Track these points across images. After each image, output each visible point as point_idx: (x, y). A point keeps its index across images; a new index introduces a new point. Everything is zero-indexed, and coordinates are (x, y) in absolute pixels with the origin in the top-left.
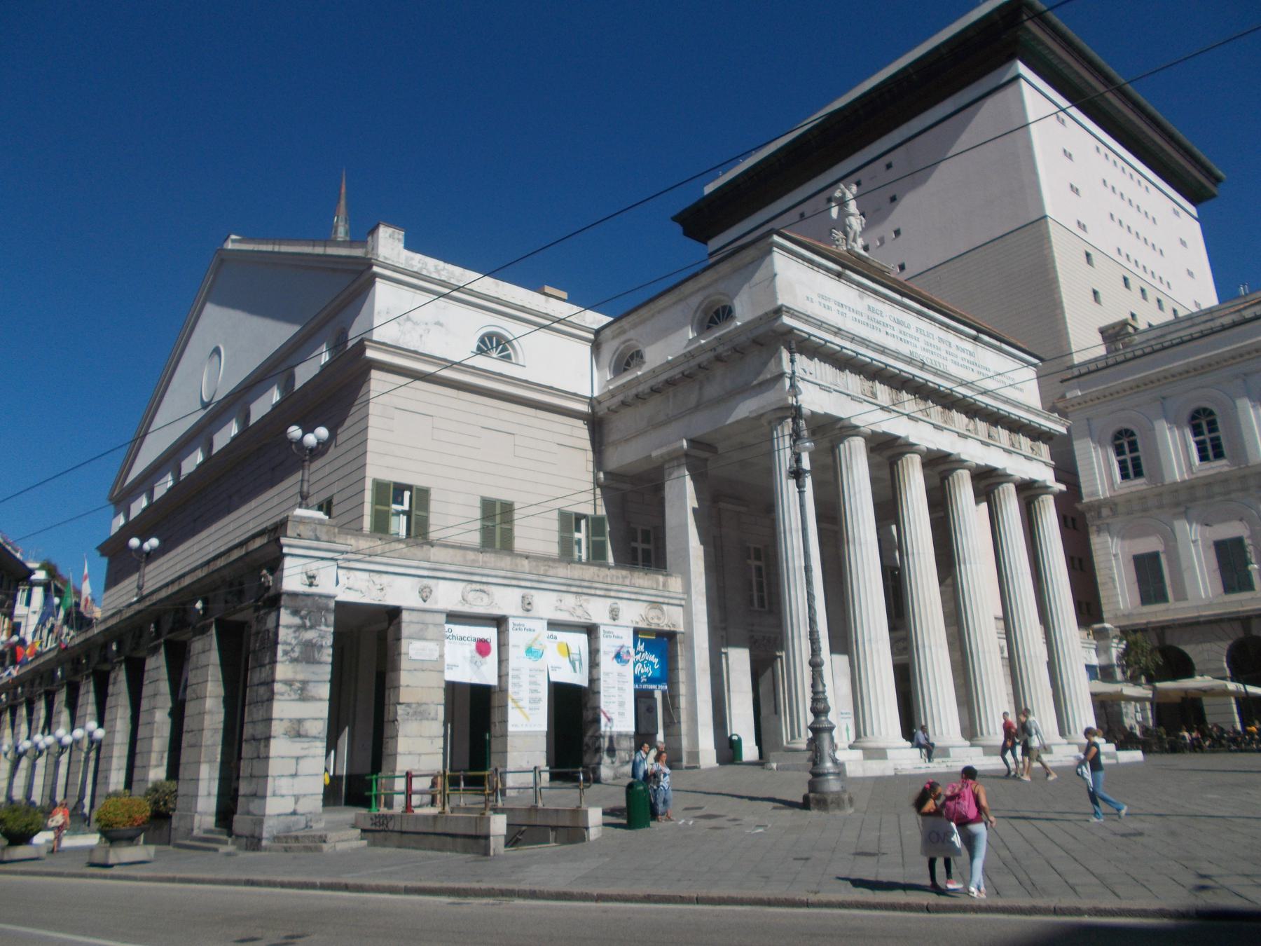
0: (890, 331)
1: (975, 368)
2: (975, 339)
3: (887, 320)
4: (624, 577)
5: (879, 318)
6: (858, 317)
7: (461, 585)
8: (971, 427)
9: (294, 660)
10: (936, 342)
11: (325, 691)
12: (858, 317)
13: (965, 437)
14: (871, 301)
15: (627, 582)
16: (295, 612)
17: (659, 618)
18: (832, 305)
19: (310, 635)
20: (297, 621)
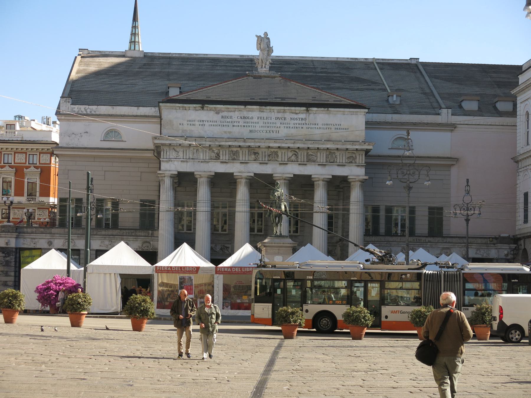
0: (235, 124)
1: (304, 126)
2: (307, 110)
3: (235, 119)
4: (132, 233)
5: (228, 120)
6: (213, 124)
7: (62, 240)
8: (293, 158)
9: (3, 266)
10: (274, 120)
11: (13, 274)
12: (213, 124)
13: (287, 164)
14: (225, 114)
15: (134, 234)
16: (3, 253)
17: (148, 247)
18: (197, 123)
19: (8, 259)
20: (4, 255)
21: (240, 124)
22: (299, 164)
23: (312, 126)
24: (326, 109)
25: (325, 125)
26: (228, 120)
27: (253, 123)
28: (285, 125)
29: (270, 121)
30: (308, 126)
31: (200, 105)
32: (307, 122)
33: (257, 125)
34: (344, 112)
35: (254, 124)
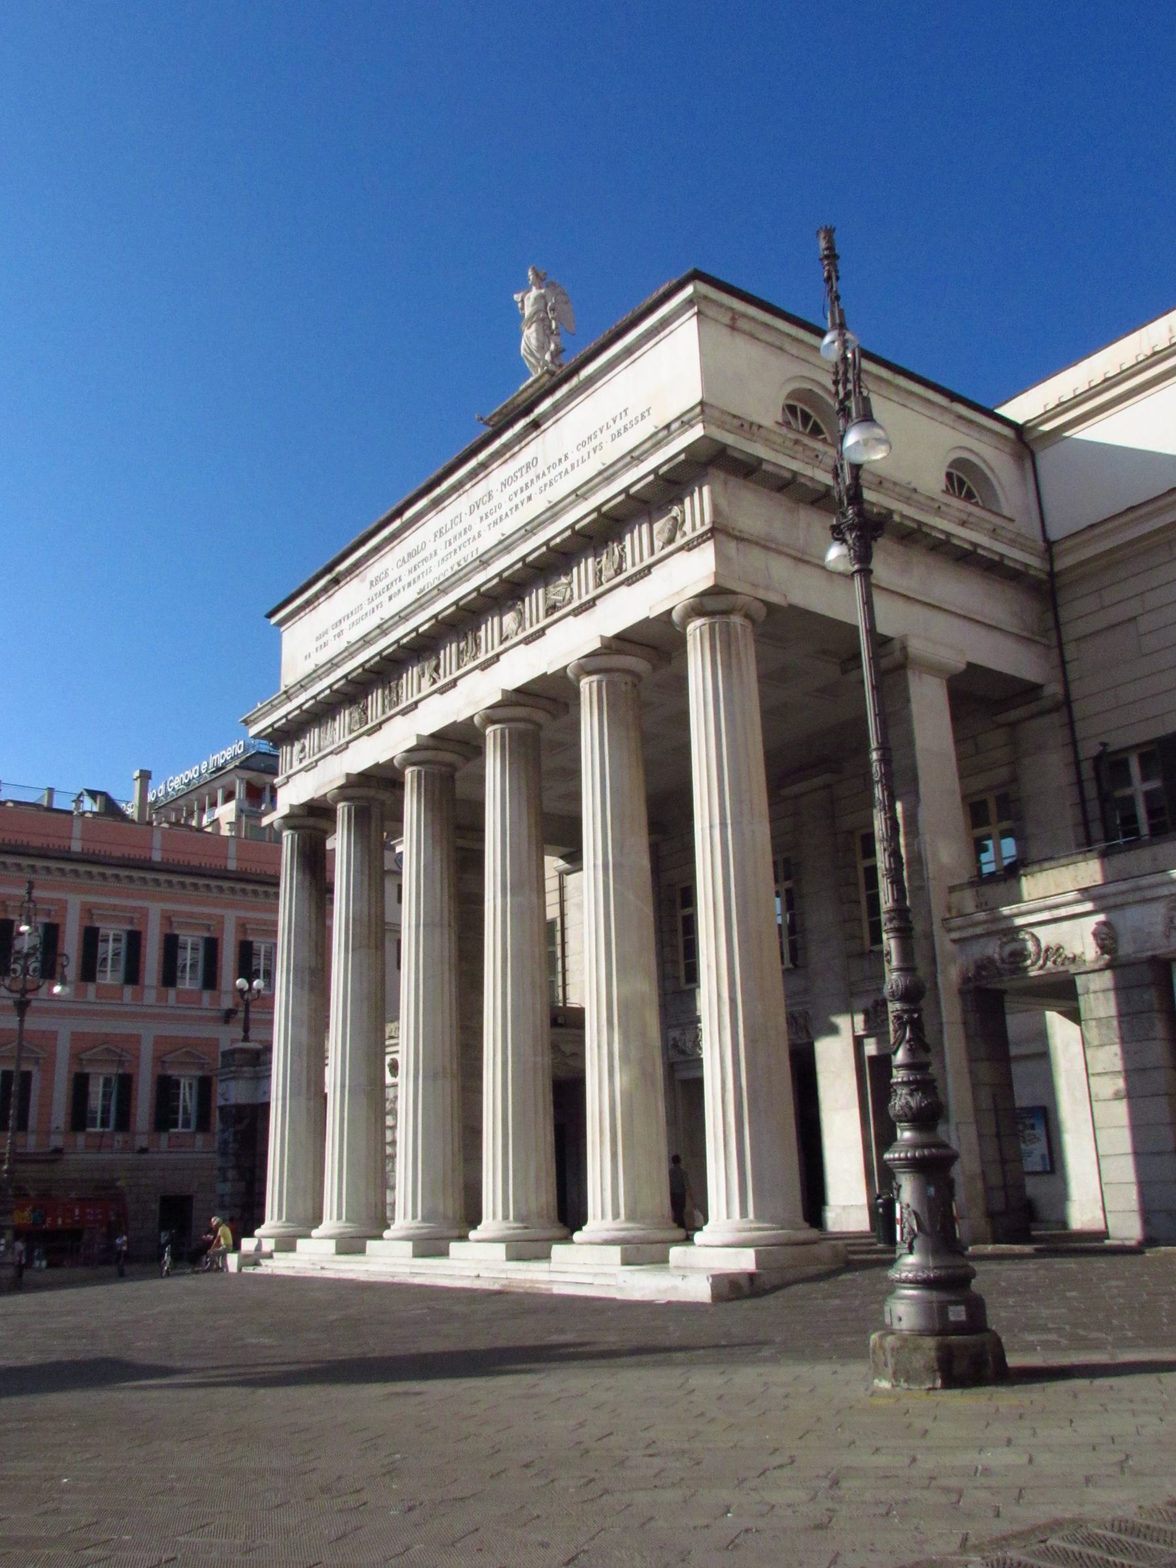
11: (231, 1174)
19: (227, 1134)
21: (399, 585)
22: (528, 641)
23: (554, 472)
24: (574, 381)
25: (583, 444)
26: (382, 585)
27: (425, 560)
28: (491, 519)
29: (459, 528)
30: (541, 482)
31: (328, 577)
32: (541, 467)
33: (433, 562)
34: (629, 351)
35: (426, 566)
